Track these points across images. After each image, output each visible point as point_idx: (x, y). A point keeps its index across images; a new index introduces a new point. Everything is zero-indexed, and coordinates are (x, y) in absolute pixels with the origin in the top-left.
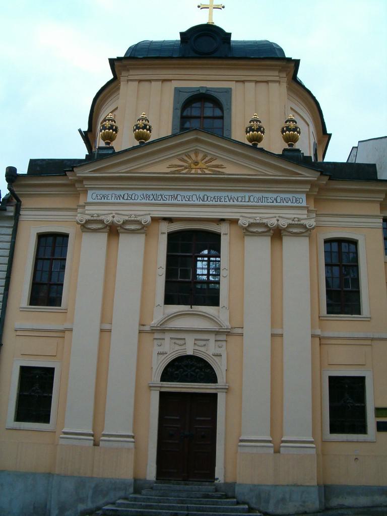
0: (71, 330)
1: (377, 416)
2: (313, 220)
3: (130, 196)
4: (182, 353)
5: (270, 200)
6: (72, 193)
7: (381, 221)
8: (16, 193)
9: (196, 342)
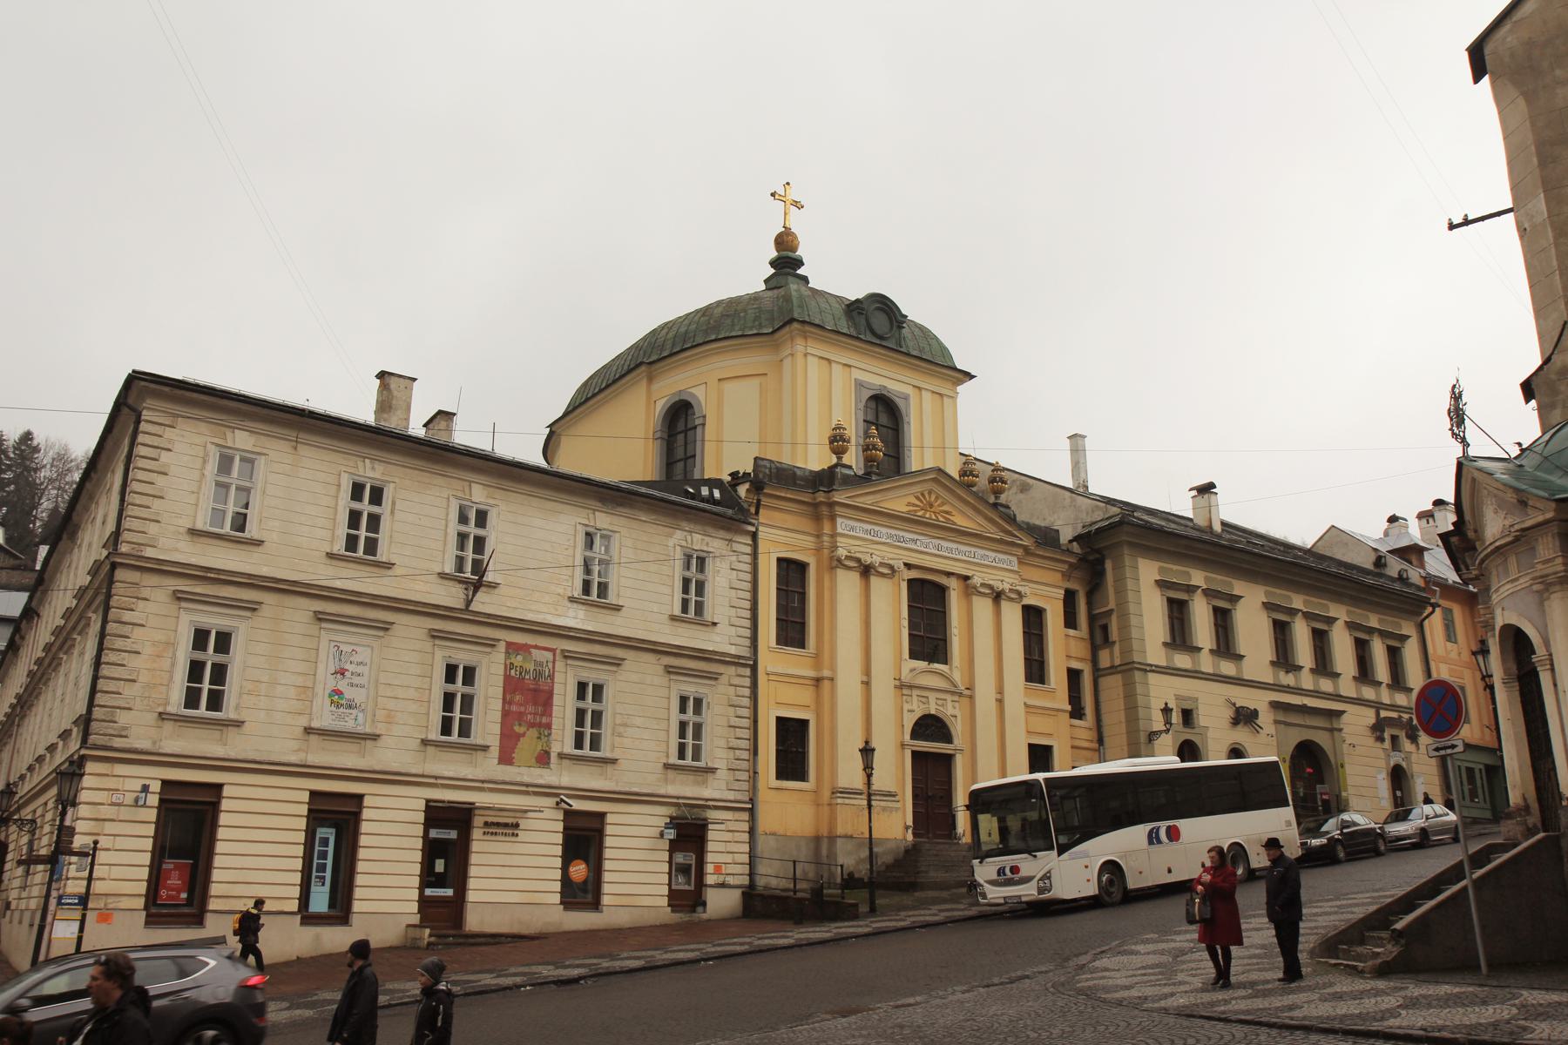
4: (927, 713)
7: (1063, 592)
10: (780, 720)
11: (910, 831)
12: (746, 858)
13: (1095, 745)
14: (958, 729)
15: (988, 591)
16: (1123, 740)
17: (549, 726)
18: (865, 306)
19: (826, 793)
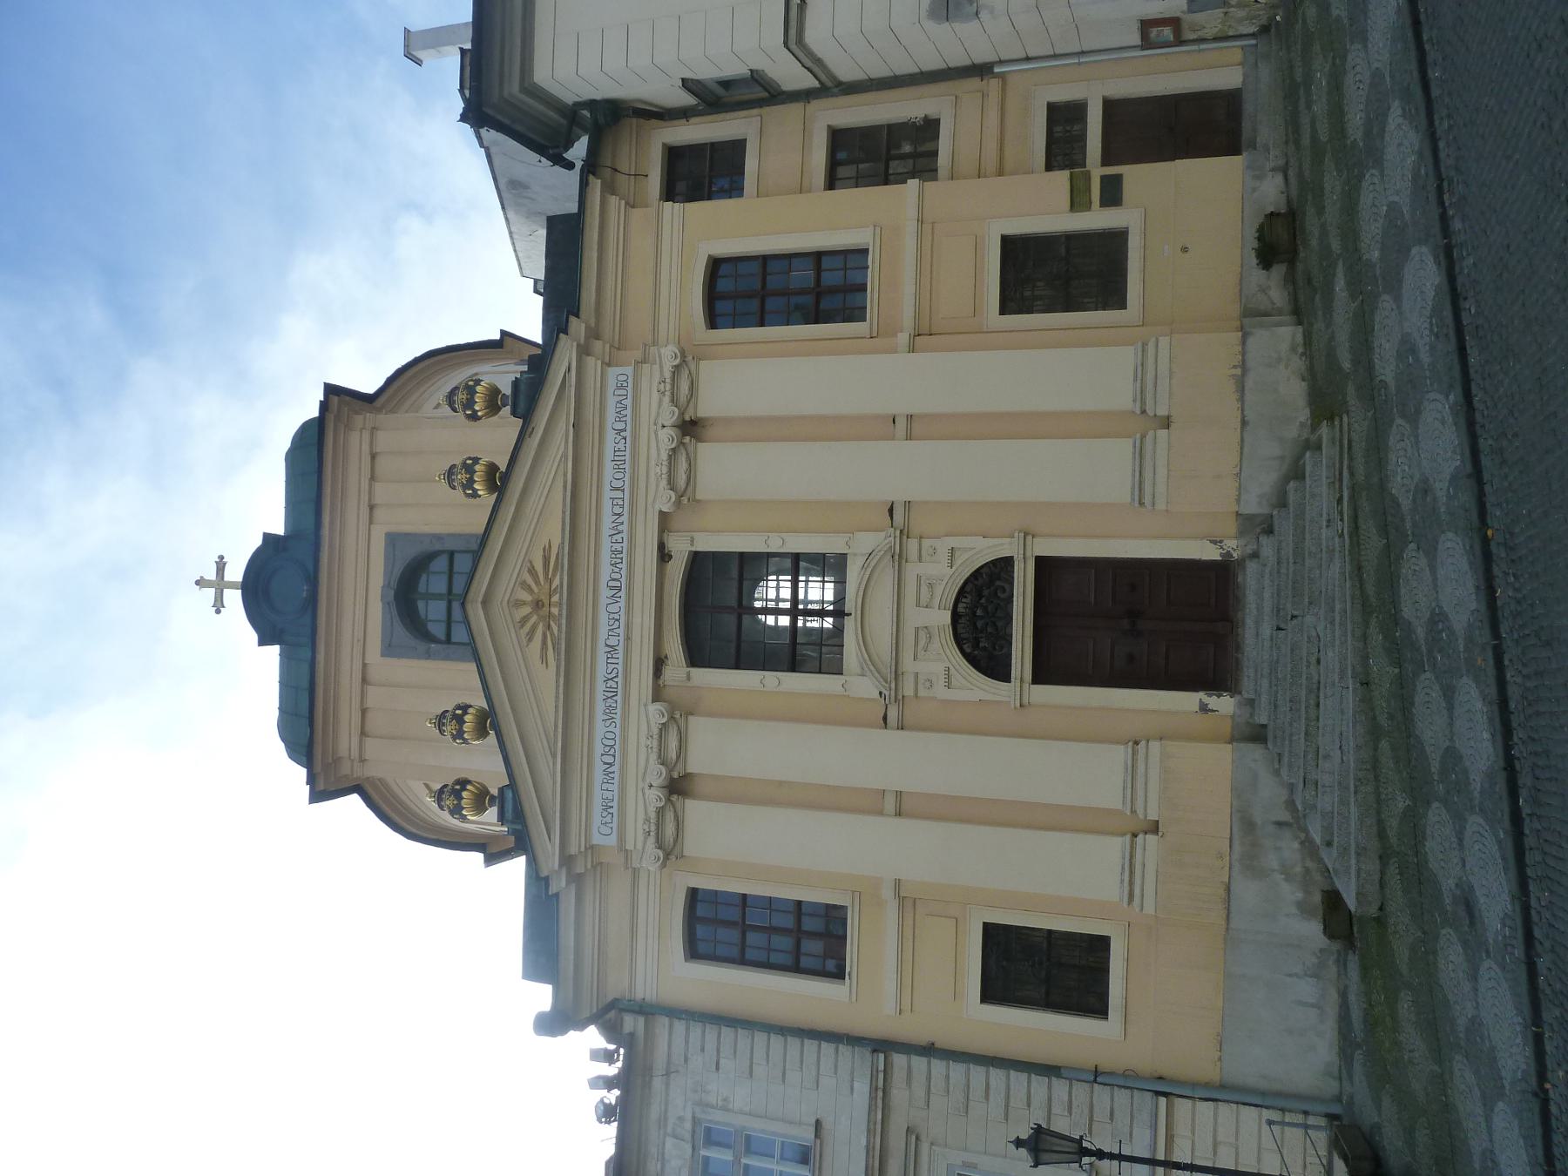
0: (898, 884)
1: (1088, 206)
2: (663, 351)
3: (607, 749)
6: (598, 879)
8: (595, 1011)
9: (924, 601)
14: (983, 551)
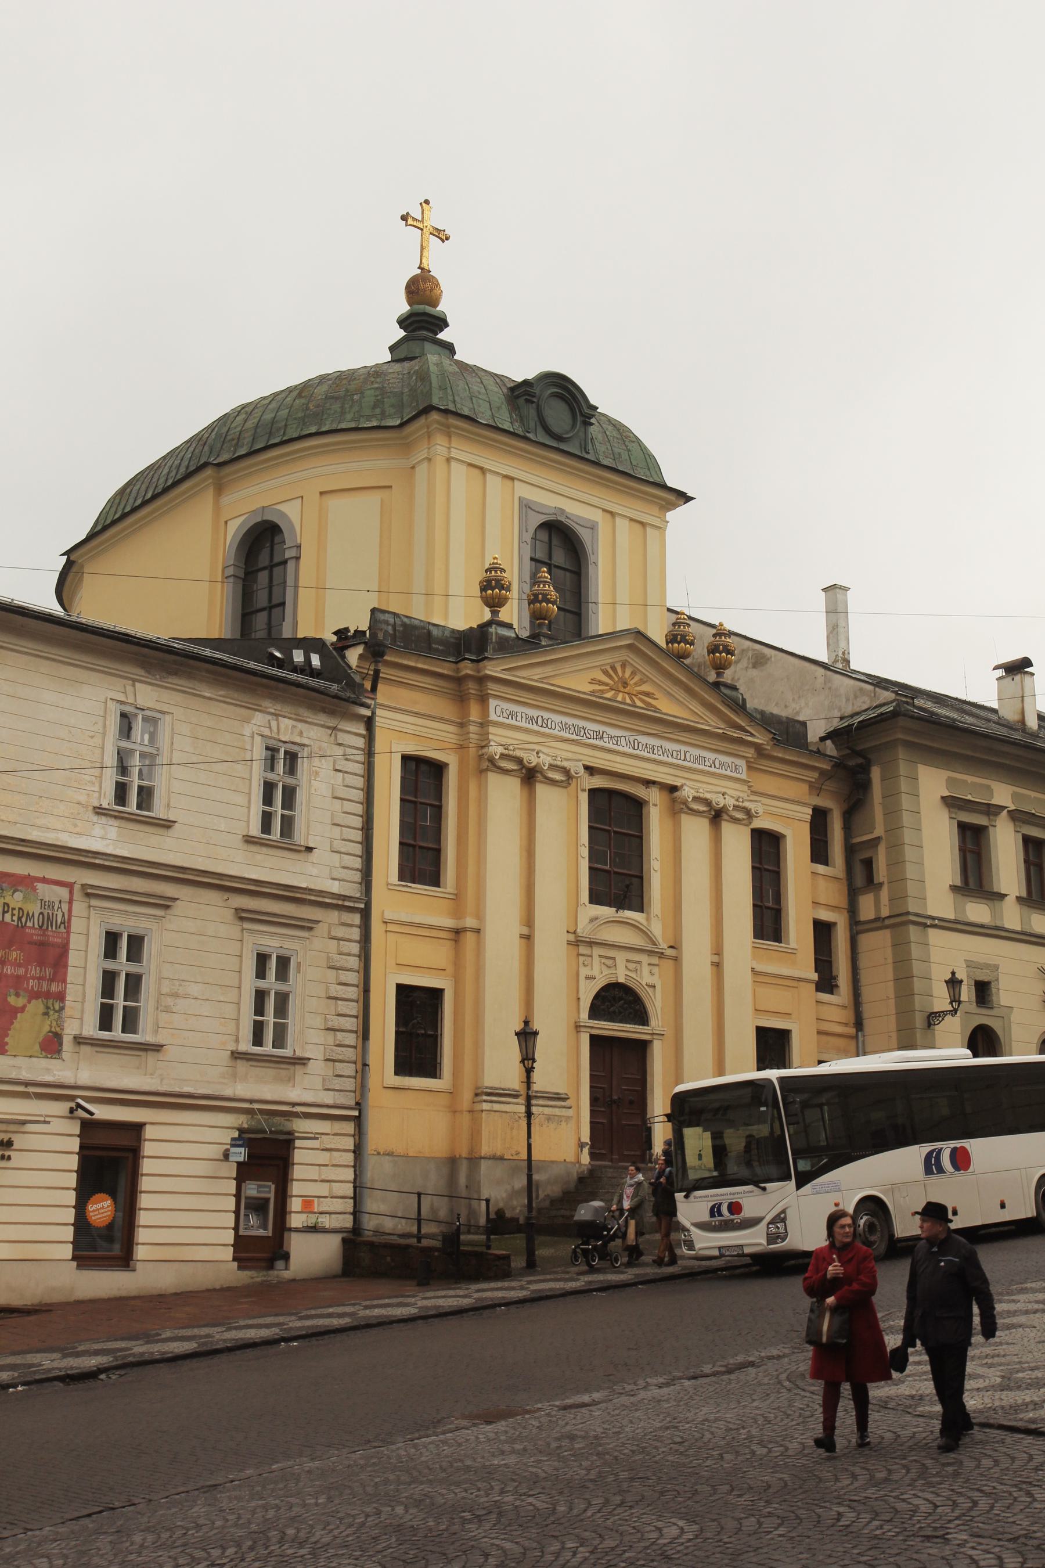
5: (707, 763)
6: (445, 690)
7: (810, 811)
10: (403, 990)
11: (586, 1150)
12: (348, 1190)
13: (852, 1031)
14: (657, 1005)
15: (702, 808)
16: (892, 1024)
17: (61, 997)
18: (537, 390)
19: (467, 1095)
